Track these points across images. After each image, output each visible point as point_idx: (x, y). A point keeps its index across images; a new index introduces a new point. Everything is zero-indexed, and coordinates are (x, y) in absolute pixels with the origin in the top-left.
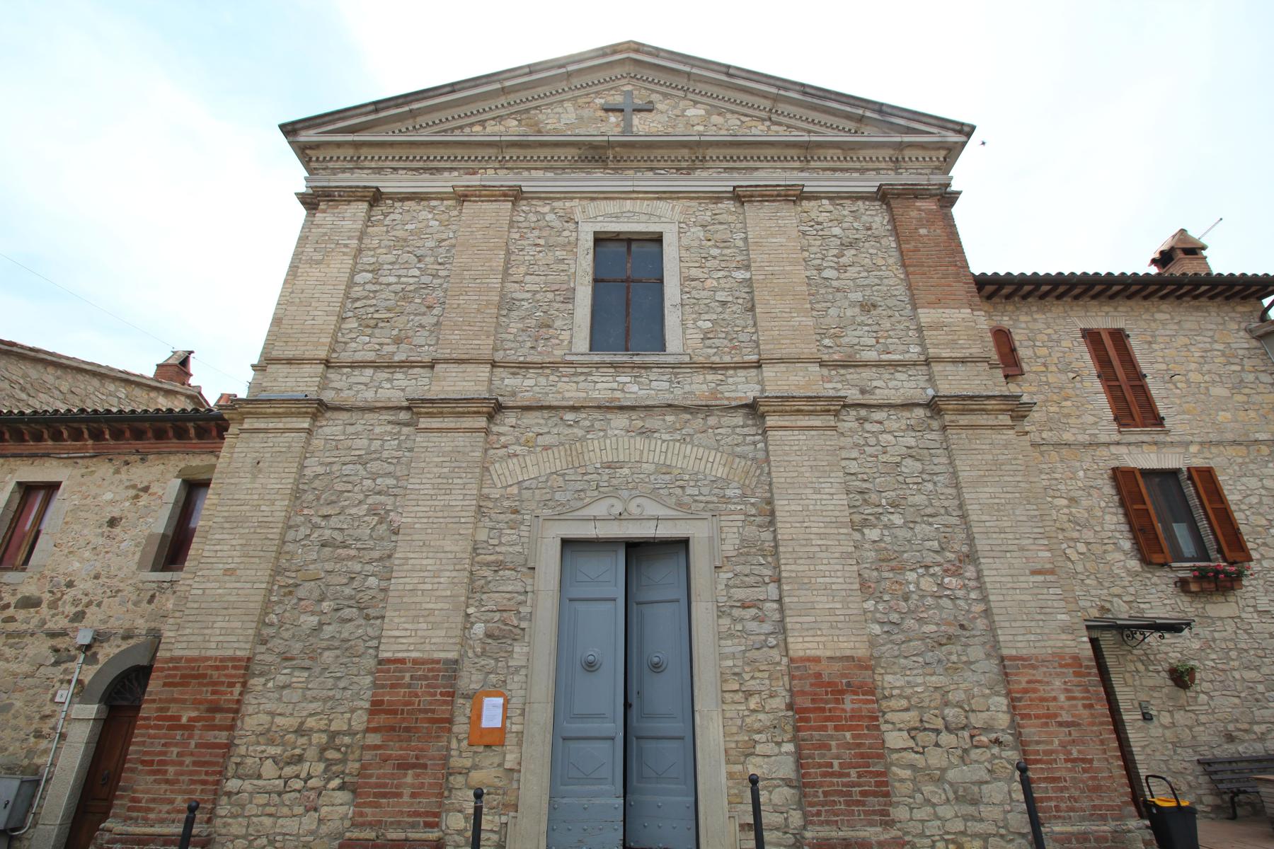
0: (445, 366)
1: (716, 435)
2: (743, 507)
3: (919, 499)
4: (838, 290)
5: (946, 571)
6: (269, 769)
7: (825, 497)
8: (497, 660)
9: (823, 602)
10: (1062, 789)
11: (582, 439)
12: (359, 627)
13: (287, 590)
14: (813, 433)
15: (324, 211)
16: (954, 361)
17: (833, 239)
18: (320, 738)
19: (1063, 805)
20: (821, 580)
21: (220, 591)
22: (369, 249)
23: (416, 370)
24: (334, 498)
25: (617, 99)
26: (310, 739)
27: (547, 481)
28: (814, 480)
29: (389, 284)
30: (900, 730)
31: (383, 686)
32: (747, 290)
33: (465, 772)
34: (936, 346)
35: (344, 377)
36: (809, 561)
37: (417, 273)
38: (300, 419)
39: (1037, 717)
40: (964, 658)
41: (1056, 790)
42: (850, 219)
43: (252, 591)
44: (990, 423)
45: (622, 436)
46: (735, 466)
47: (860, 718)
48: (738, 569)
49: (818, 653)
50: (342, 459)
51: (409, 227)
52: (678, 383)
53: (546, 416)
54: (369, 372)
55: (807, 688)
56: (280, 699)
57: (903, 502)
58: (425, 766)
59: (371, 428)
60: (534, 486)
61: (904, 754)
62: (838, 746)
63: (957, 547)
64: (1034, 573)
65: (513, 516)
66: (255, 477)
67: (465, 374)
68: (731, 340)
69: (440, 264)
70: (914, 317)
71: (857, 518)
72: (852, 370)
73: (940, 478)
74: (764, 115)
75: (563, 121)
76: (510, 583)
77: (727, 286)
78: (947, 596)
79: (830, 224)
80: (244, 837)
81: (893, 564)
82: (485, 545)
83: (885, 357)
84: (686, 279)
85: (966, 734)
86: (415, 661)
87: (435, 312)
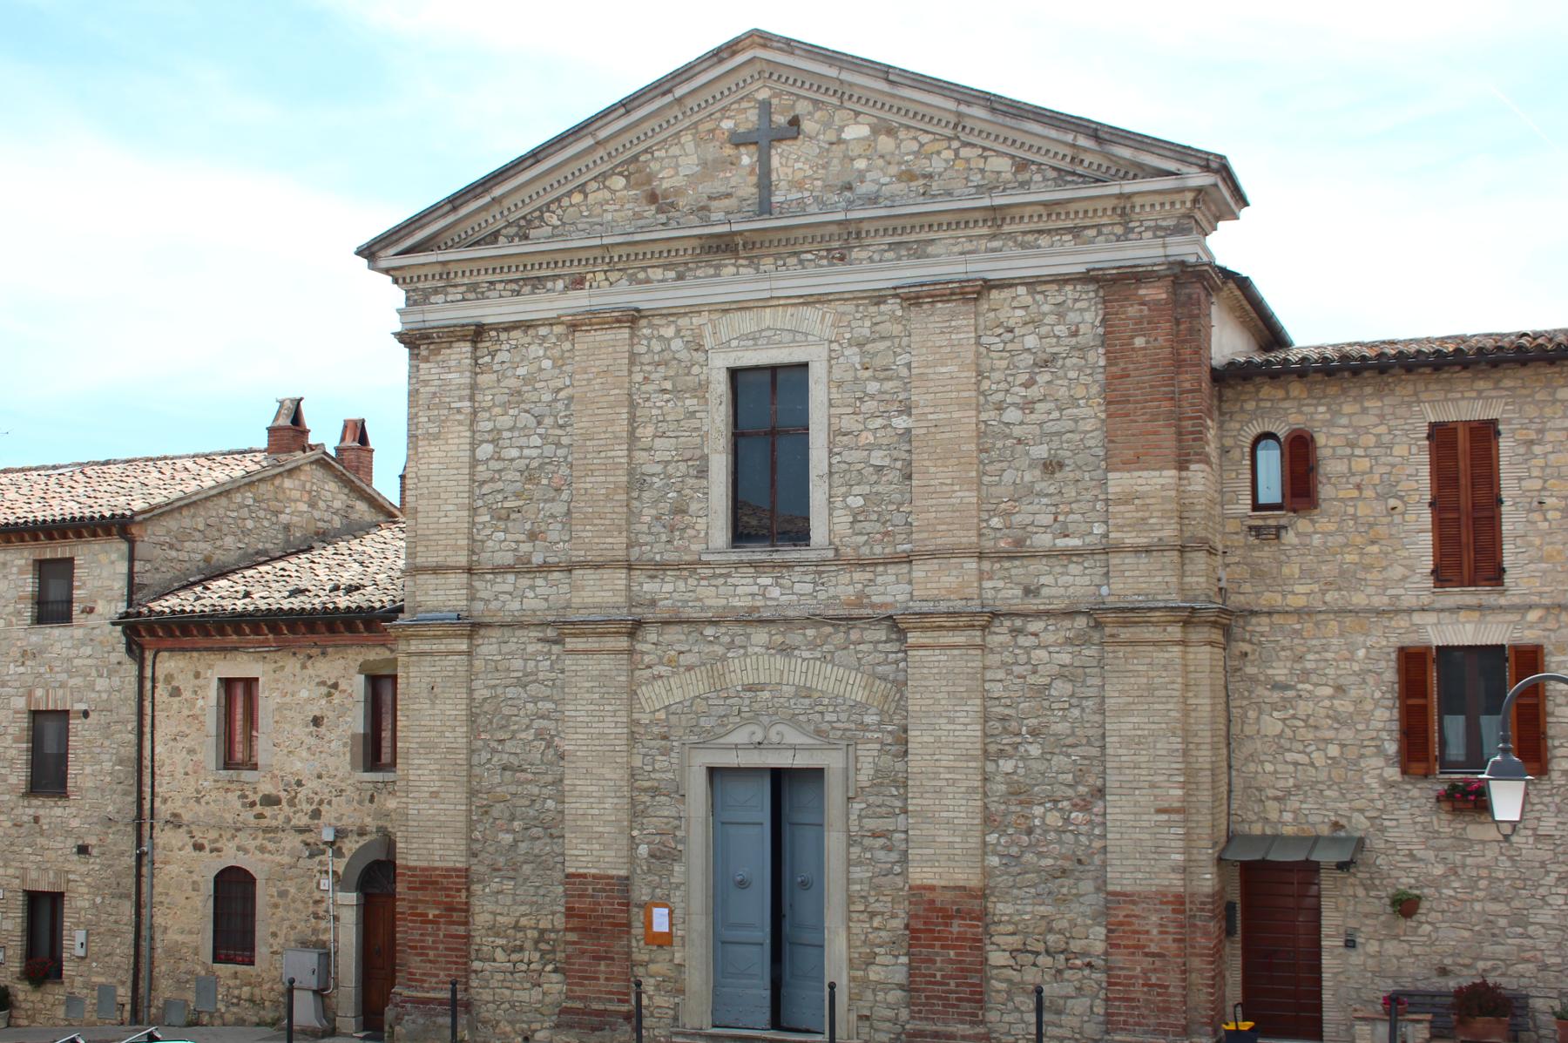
0: (581, 572)
1: (857, 652)
2: (880, 735)
3: (1062, 728)
4: (1020, 441)
5: (1075, 805)
7: (958, 727)
8: (660, 876)
9: (944, 836)
10: (1133, 1008)
11: (724, 658)
12: (546, 844)
14: (956, 652)
15: (427, 360)
16: (1137, 550)
17: (1025, 355)
18: (534, 934)
19: (1131, 1020)
20: (945, 814)
22: (484, 410)
23: (556, 575)
25: (749, 119)
27: (691, 705)
28: (950, 708)
29: (512, 460)
30: (1004, 950)
31: (573, 896)
32: (907, 447)
33: (645, 964)
34: (1120, 528)
36: (935, 795)
37: (539, 442)
39: (1126, 947)
40: (1074, 891)
41: (1127, 1008)
42: (1051, 319)
44: (1157, 637)
45: (762, 655)
46: (875, 689)
47: (965, 939)
48: (871, 799)
49: (934, 882)
51: (521, 371)
52: (823, 584)
53: (686, 630)
54: (511, 578)
55: (921, 913)
56: (497, 902)
57: (1044, 730)
58: (612, 959)
59: (523, 646)
60: (679, 711)
61: (1004, 970)
62: (942, 961)
63: (1091, 781)
64: (1160, 811)
66: (433, 703)
67: (602, 582)
68: (884, 523)
69: (561, 427)
70: (1103, 483)
71: (993, 748)
72: (1017, 563)
73: (1090, 703)
74: (949, 132)
75: (683, 171)
76: (665, 809)
77: (885, 441)
78: (1071, 831)
79: (1023, 331)
80: (494, 1002)
81: (1023, 797)
82: (641, 771)
83: (1062, 543)
84: (835, 433)
85: (1062, 957)
86: (594, 876)
87: (565, 496)
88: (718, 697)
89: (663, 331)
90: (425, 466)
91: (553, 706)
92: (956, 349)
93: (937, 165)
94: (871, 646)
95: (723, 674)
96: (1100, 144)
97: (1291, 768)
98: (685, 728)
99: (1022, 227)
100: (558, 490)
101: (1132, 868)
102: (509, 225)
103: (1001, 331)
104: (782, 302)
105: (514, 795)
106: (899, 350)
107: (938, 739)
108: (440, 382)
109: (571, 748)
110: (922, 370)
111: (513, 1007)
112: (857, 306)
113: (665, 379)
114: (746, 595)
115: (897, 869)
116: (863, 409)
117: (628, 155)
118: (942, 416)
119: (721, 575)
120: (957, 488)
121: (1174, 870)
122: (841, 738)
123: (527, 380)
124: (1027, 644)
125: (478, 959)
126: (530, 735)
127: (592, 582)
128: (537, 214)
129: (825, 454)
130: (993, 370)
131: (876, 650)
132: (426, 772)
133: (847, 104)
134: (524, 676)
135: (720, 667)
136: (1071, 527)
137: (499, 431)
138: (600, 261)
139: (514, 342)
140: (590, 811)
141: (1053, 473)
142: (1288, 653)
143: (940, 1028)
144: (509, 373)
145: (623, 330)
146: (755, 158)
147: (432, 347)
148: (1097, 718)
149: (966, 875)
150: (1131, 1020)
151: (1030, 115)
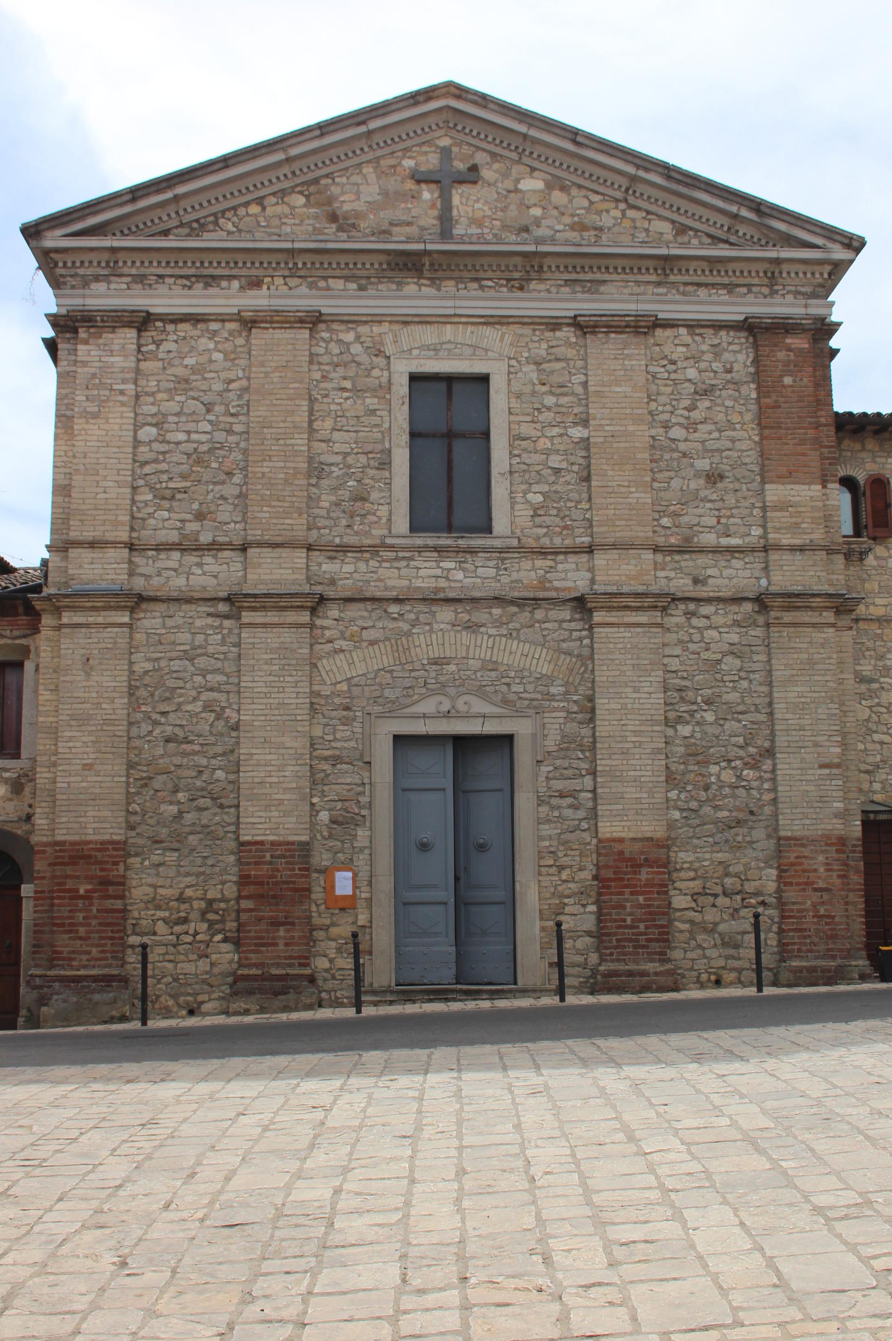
0: (258, 550)
1: (542, 630)
2: (565, 704)
3: (733, 697)
4: (685, 455)
5: (746, 764)
6: (161, 927)
7: (643, 696)
8: (343, 842)
9: (631, 792)
10: (805, 937)
11: (408, 634)
12: (215, 814)
13: (142, 782)
14: (639, 630)
15: (86, 342)
16: (793, 549)
17: (687, 384)
19: (804, 948)
21: (84, 784)
22: (147, 394)
23: (227, 554)
24: (167, 694)
25: (430, 161)
26: (191, 906)
27: (375, 678)
28: (635, 679)
29: (178, 443)
30: (685, 894)
31: (248, 864)
32: (584, 454)
33: (326, 928)
34: (777, 530)
35: (150, 561)
36: (622, 756)
37: (208, 428)
38: (119, 613)
39: (798, 884)
40: (748, 839)
41: (799, 937)
42: (708, 357)
43: (114, 784)
44: (814, 620)
45: (448, 631)
46: (560, 663)
47: (653, 885)
48: (558, 762)
49: (623, 835)
50: (168, 654)
51: (189, 361)
52: (506, 569)
53: (369, 607)
54: (176, 555)
55: (611, 863)
56: (158, 875)
57: (717, 700)
58: (293, 924)
59: (191, 621)
61: (686, 912)
62: (632, 907)
63: (759, 743)
64: (822, 766)
65: (345, 713)
66: (88, 675)
67: (282, 560)
68: (563, 518)
69: (232, 415)
70: (762, 492)
71: (672, 715)
72: (687, 556)
73: (757, 676)
74: (619, 195)
75: (364, 199)
76: (349, 776)
77: (562, 447)
78: (744, 787)
79: (685, 364)
81: (700, 758)
82: (321, 741)
83: (724, 541)
84: (516, 438)
85: (739, 897)
86: (273, 843)
87: (237, 479)
88: (403, 670)
89: (342, 336)
90: (82, 443)
91: (225, 679)
92: (629, 373)
93: (606, 221)
94: (556, 625)
95: (409, 649)
96: (760, 217)
97: (878, 747)
98: (369, 699)
99: (687, 279)
100: (229, 474)
101: (800, 816)
102: (182, 225)
103: (665, 362)
104: (464, 320)
105: (179, 766)
106: (574, 371)
107: (624, 706)
108: (101, 364)
109: (248, 718)
110: (598, 389)
111: (176, 980)
112: (534, 330)
113: (345, 378)
114: (429, 577)
115: (584, 825)
116: (541, 418)
117: (311, 176)
118: (618, 428)
119: (404, 558)
120: (633, 490)
121: (836, 816)
122: (528, 707)
123: (194, 370)
124: (700, 625)
125: (135, 933)
126: (198, 707)
127: (269, 560)
128: (211, 219)
129: (507, 456)
130: (658, 394)
131: (560, 628)
132: (79, 744)
133: (525, 160)
134: (192, 649)
135: (405, 642)
136: (733, 529)
137: (165, 415)
138: (283, 265)
139: (182, 334)
140: (268, 779)
141: (715, 483)
142: (872, 653)
143: (631, 967)
144: (177, 362)
145: (303, 331)
146: (436, 195)
147: (92, 330)
148: (765, 689)
149: (652, 828)
150: (804, 948)
151: (702, 186)
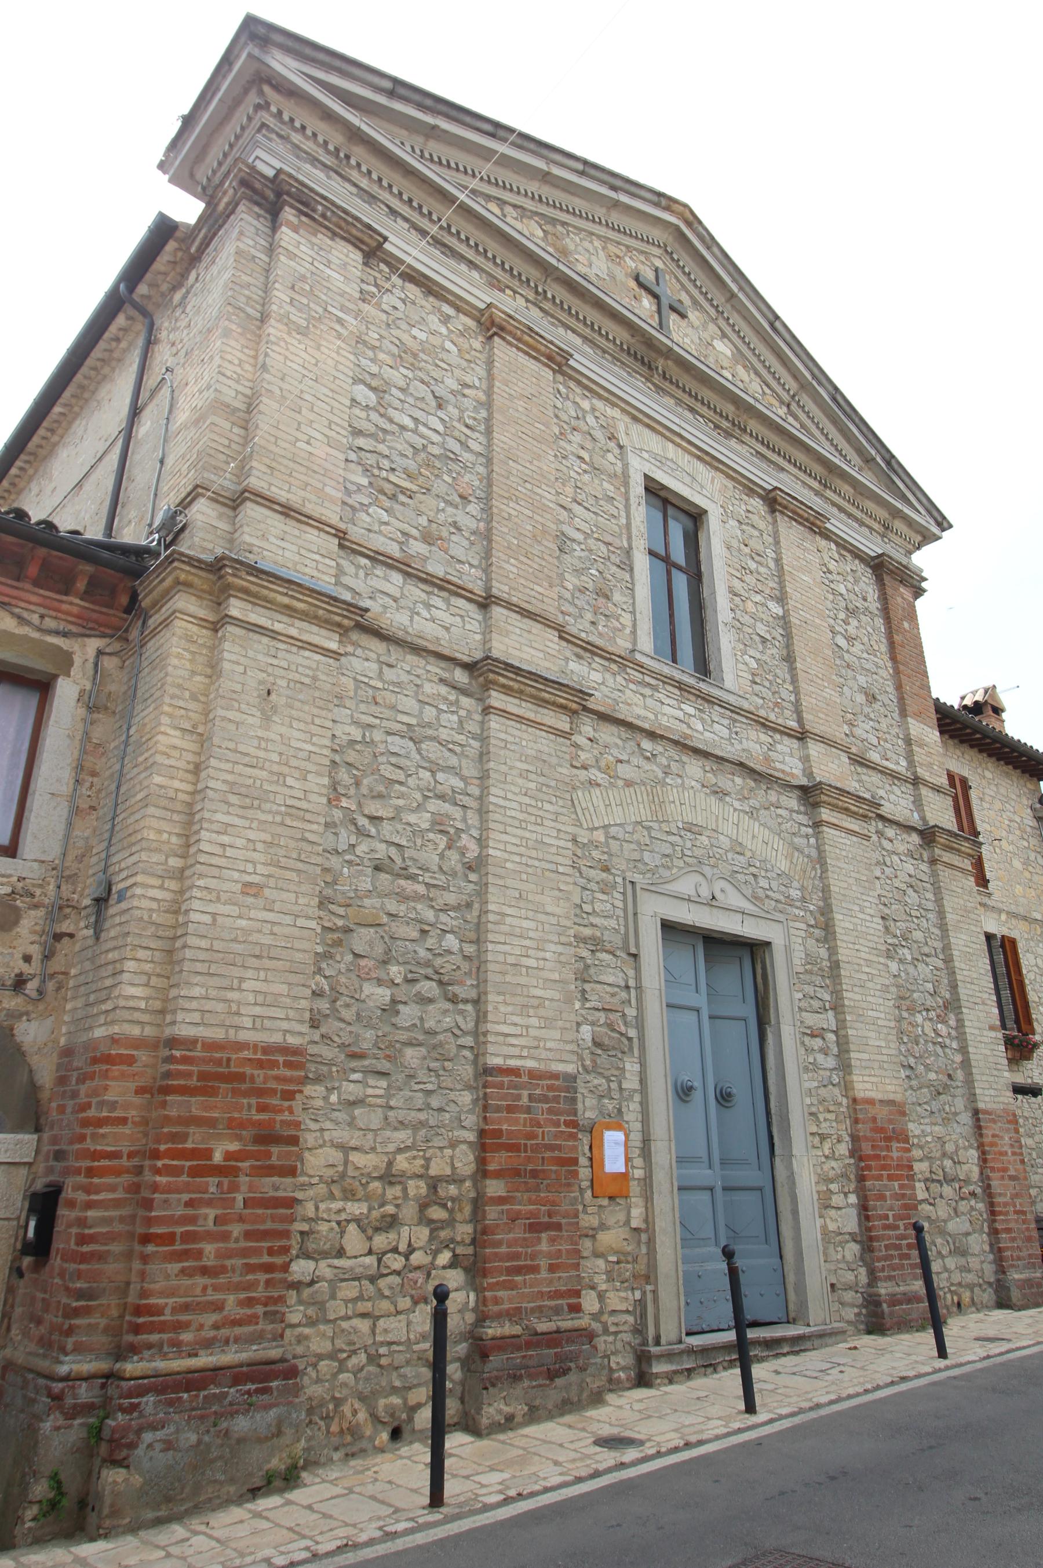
0: (505, 612)
6: (354, 1240)
8: (609, 1081)
13: (335, 936)
18: (417, 1188)
20: (870, 1013)
21: (243, 923)
23: (461, 602)
24: (381, 788)
26: (405, 1190)
29: (403, 428)
35: (361, 573)
38: (323, 632)
43: (296, 932)
50: (385, 723)
53: (624, 735)
54: (397, 578)
56: (352, 1124)
58: (558, 1227)
60: (620, 836)
65: (604, 875)
66: (267, 719)
74: (786, 397)
80: (332, 1356)
86: (533, 1074)
91: (462, 785)
109: (498, 853)
111: (373, 1359)
126: (423, 820)
132: (240, 842)
